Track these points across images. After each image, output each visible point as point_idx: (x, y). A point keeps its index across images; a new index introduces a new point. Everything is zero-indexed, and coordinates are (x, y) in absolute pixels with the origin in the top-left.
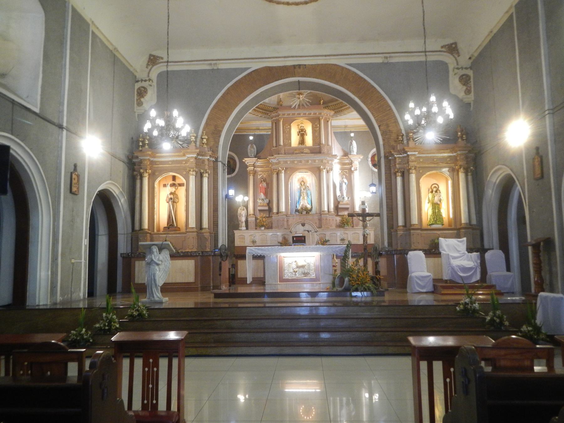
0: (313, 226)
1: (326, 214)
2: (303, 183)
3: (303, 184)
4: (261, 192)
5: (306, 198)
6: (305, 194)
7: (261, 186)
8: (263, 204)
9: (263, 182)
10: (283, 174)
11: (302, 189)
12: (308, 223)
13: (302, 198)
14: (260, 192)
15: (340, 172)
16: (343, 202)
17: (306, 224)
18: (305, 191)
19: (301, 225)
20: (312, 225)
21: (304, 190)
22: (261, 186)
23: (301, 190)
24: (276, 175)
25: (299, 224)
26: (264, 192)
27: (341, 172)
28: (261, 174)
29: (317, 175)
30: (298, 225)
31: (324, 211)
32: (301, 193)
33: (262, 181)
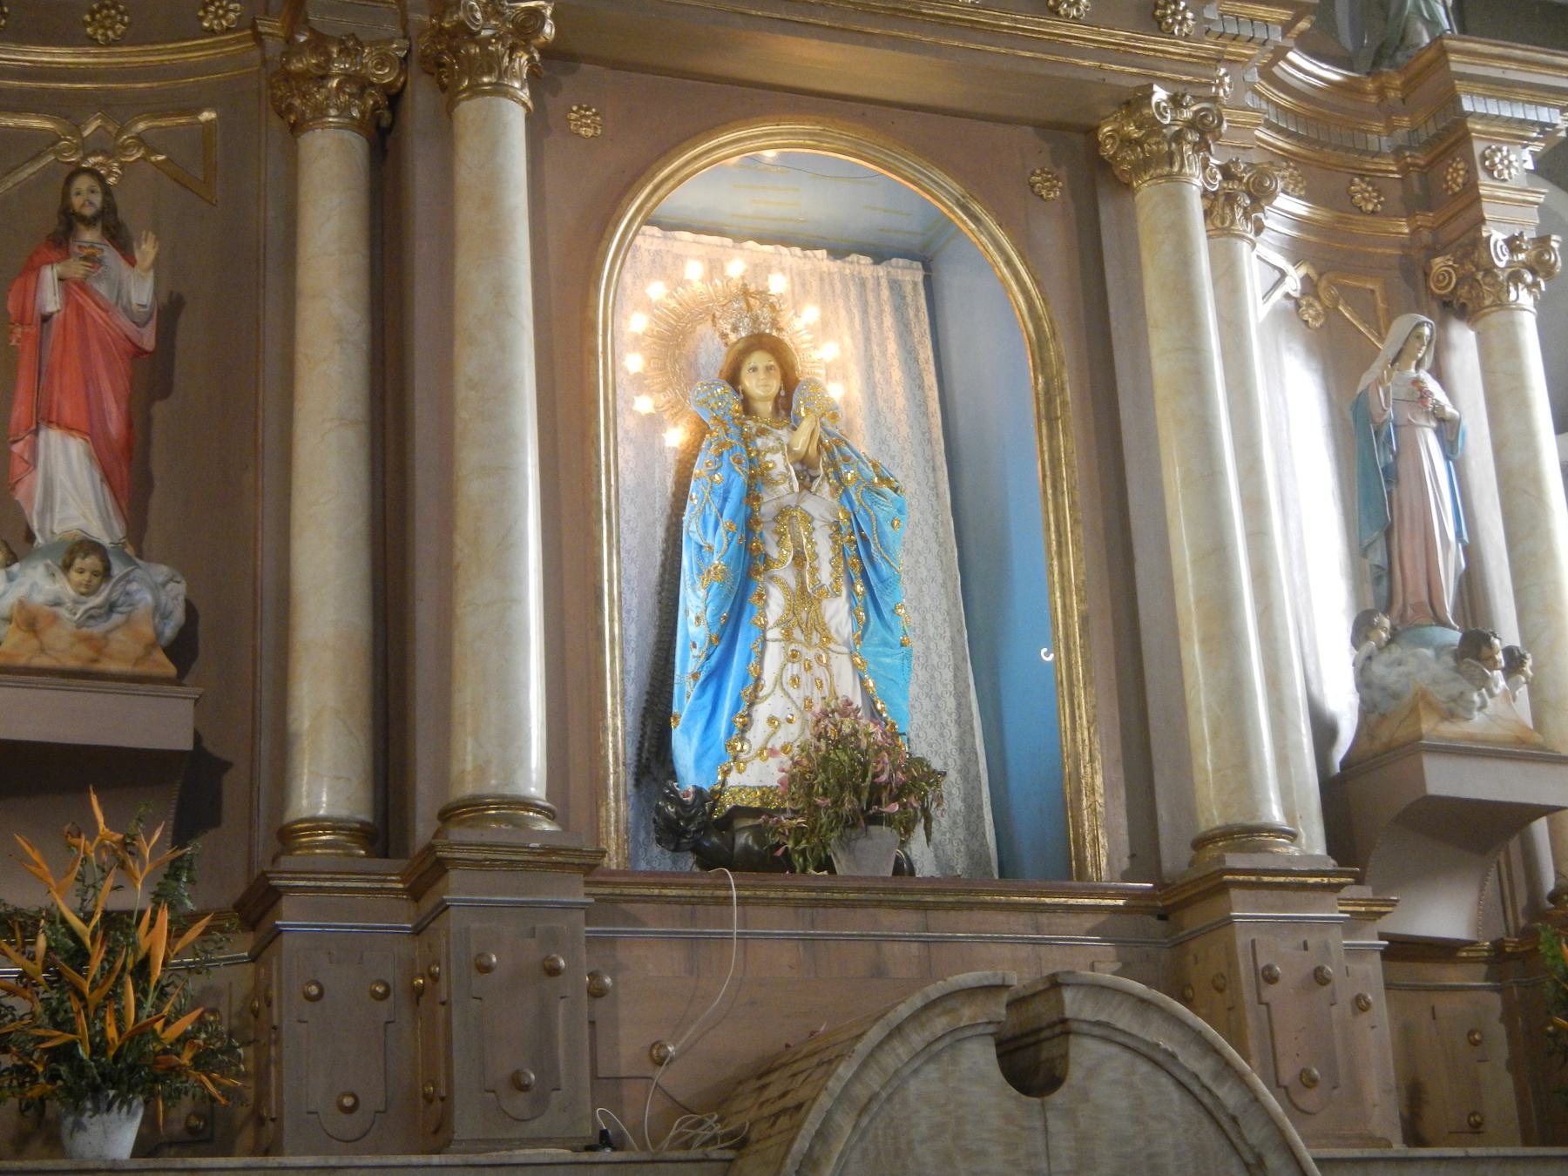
0: (1229, 1096)
1: (1293, 883)
2: (775, 385)
3: (760, 383)
4: (45, 416)
5: (838, 613)
6: (824, 548)
7: (51, 299)
8: (99, 646)
9: (89, 236)
10: (514, 117)
11: (778, 463)
12: (1124, 1019)
13: (776, 604)
14: (20, 411)
15: (1293, 284)
16: (1454, 710)
17: (1085, 1054)
18: (821, 505)
19: (981, 1057)
20: (1202, 1066)
21: (806, 470)
22: (51, 299)
23: (757, 479)
24: (357, 144)
25: (956, 1037)
26: (115, 425)
27: (1309, 285)
28: (34, 144)
29: (1053, 234)
30: (929, 1053)
31: (1249, 835)
32: (749, 525)
33: (70, 221)
